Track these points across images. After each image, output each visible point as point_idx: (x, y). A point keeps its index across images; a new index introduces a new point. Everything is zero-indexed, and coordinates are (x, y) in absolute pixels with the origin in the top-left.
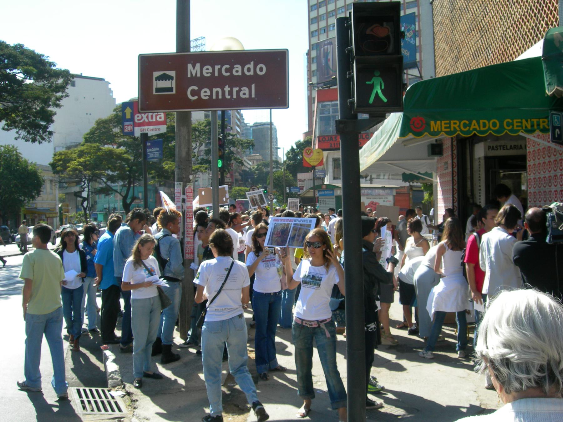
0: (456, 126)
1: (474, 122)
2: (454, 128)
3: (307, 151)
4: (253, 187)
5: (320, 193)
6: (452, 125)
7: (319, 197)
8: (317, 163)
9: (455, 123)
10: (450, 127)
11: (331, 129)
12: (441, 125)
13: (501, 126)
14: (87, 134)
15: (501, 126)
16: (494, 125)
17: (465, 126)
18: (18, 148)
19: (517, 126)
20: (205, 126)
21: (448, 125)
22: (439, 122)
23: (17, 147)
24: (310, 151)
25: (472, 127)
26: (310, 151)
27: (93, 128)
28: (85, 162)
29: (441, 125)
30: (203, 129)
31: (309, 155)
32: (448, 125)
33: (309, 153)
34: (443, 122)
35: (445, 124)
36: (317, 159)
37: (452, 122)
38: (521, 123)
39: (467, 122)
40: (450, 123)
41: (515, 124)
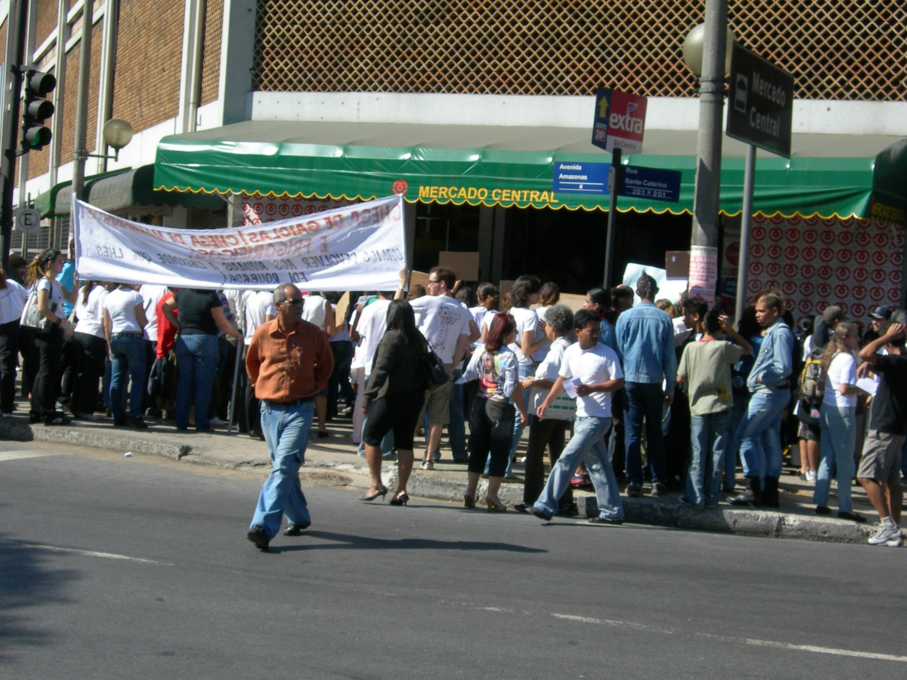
0: (444, 193)
1: (463, 189)
2: (442, 195)
6: (441, 193)
9: (443, 190)
10: (437, 194)
12: (430, 190)
13: (490, 196)
15: (490, 196)
16: (483, 194)
17: (453, 192)
19: (506, 197)
21: (436, 192)
22: (428, 188)
25: (460, 194)
29: (430, 190)
32: (436, 192)
34: (432, 188)
35: (434, 190)
37: (441, 188)
38: (511, 194)
39: (456, 189)
40: (438, 190)
41: (504, 195)
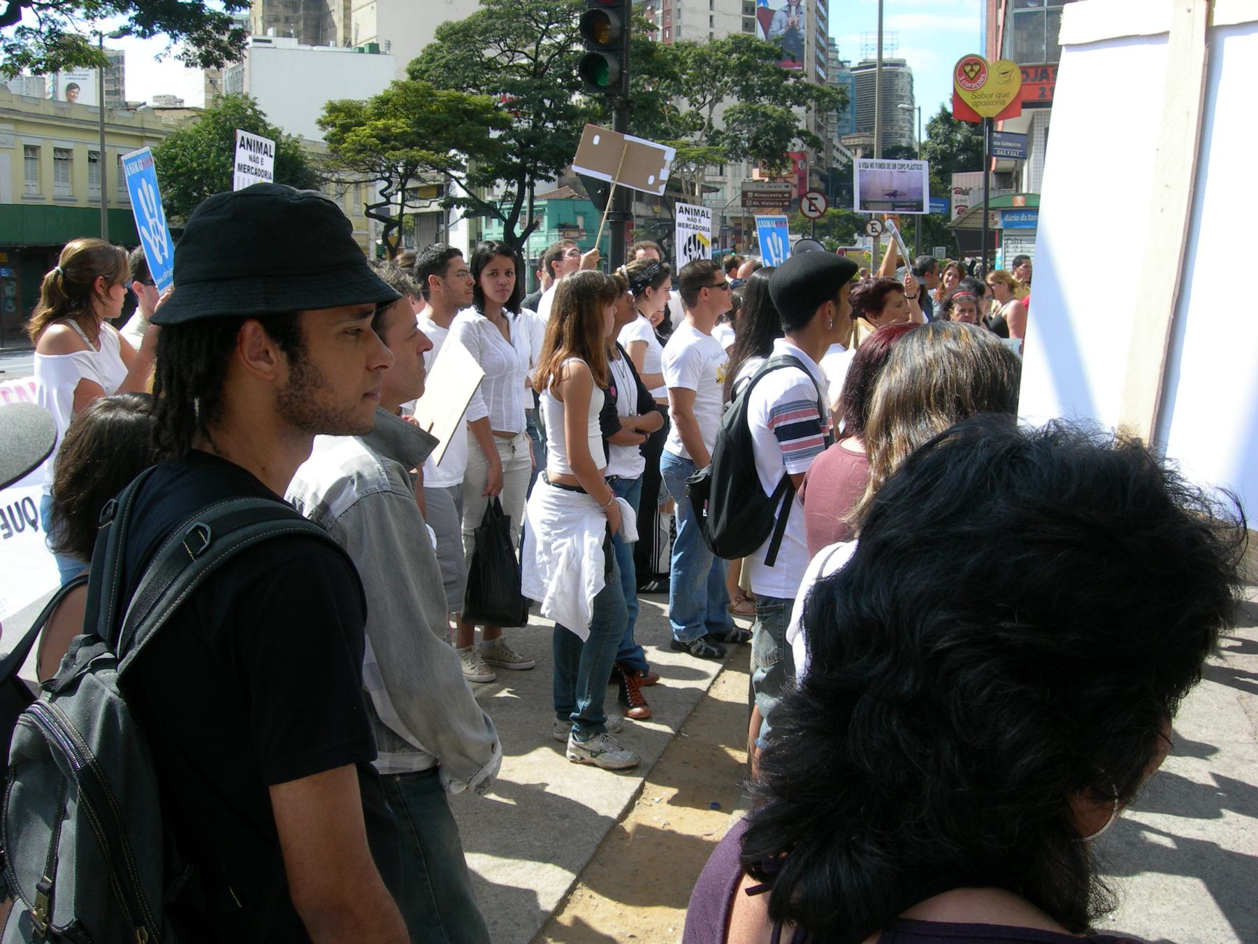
3: (968, 69)
4: (810, 195)
5: (1008, 218)
7: (1005, 232)
8: (999, 109)
11: (1044, 47)
14: (418, 61)
18: (257, 101)
20: (729, 53)
23: (255, 98)
24: (977, 68)
26: (977, 68)
27: (430, 46)
28: (387, 129)
30: (720, 59)
31: (972, 80)
33: (972, 75)
36: (999, 95)
